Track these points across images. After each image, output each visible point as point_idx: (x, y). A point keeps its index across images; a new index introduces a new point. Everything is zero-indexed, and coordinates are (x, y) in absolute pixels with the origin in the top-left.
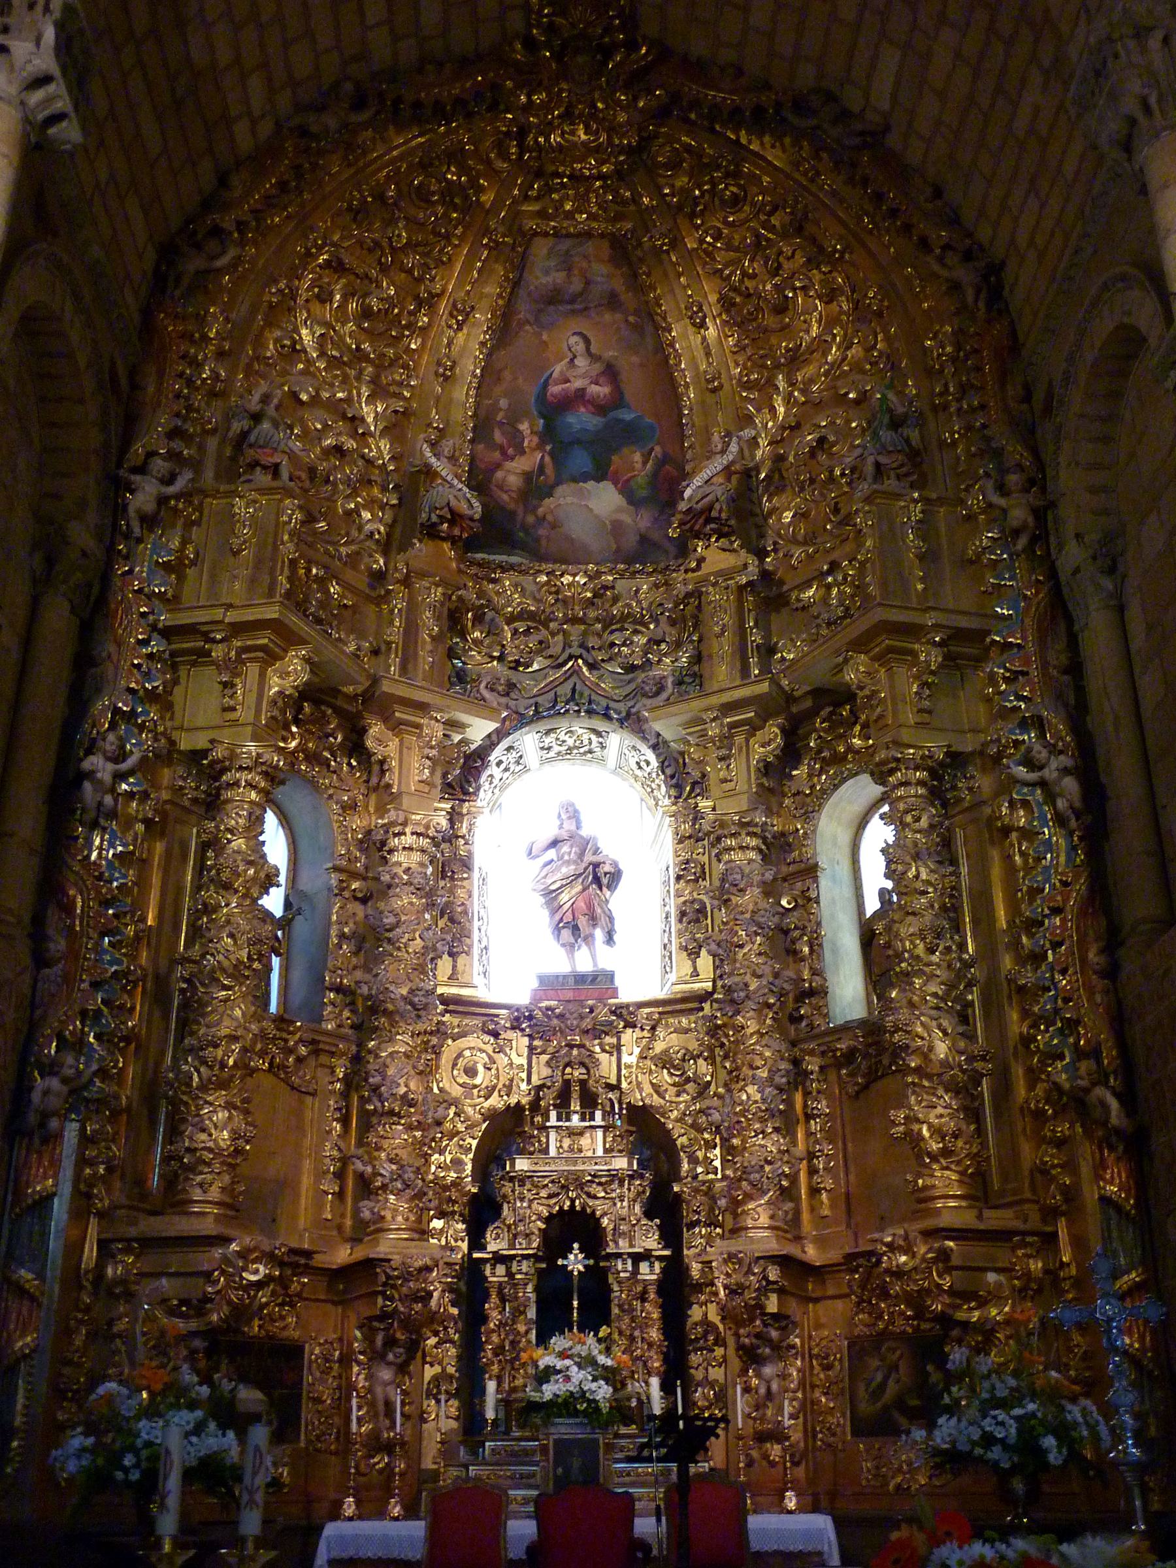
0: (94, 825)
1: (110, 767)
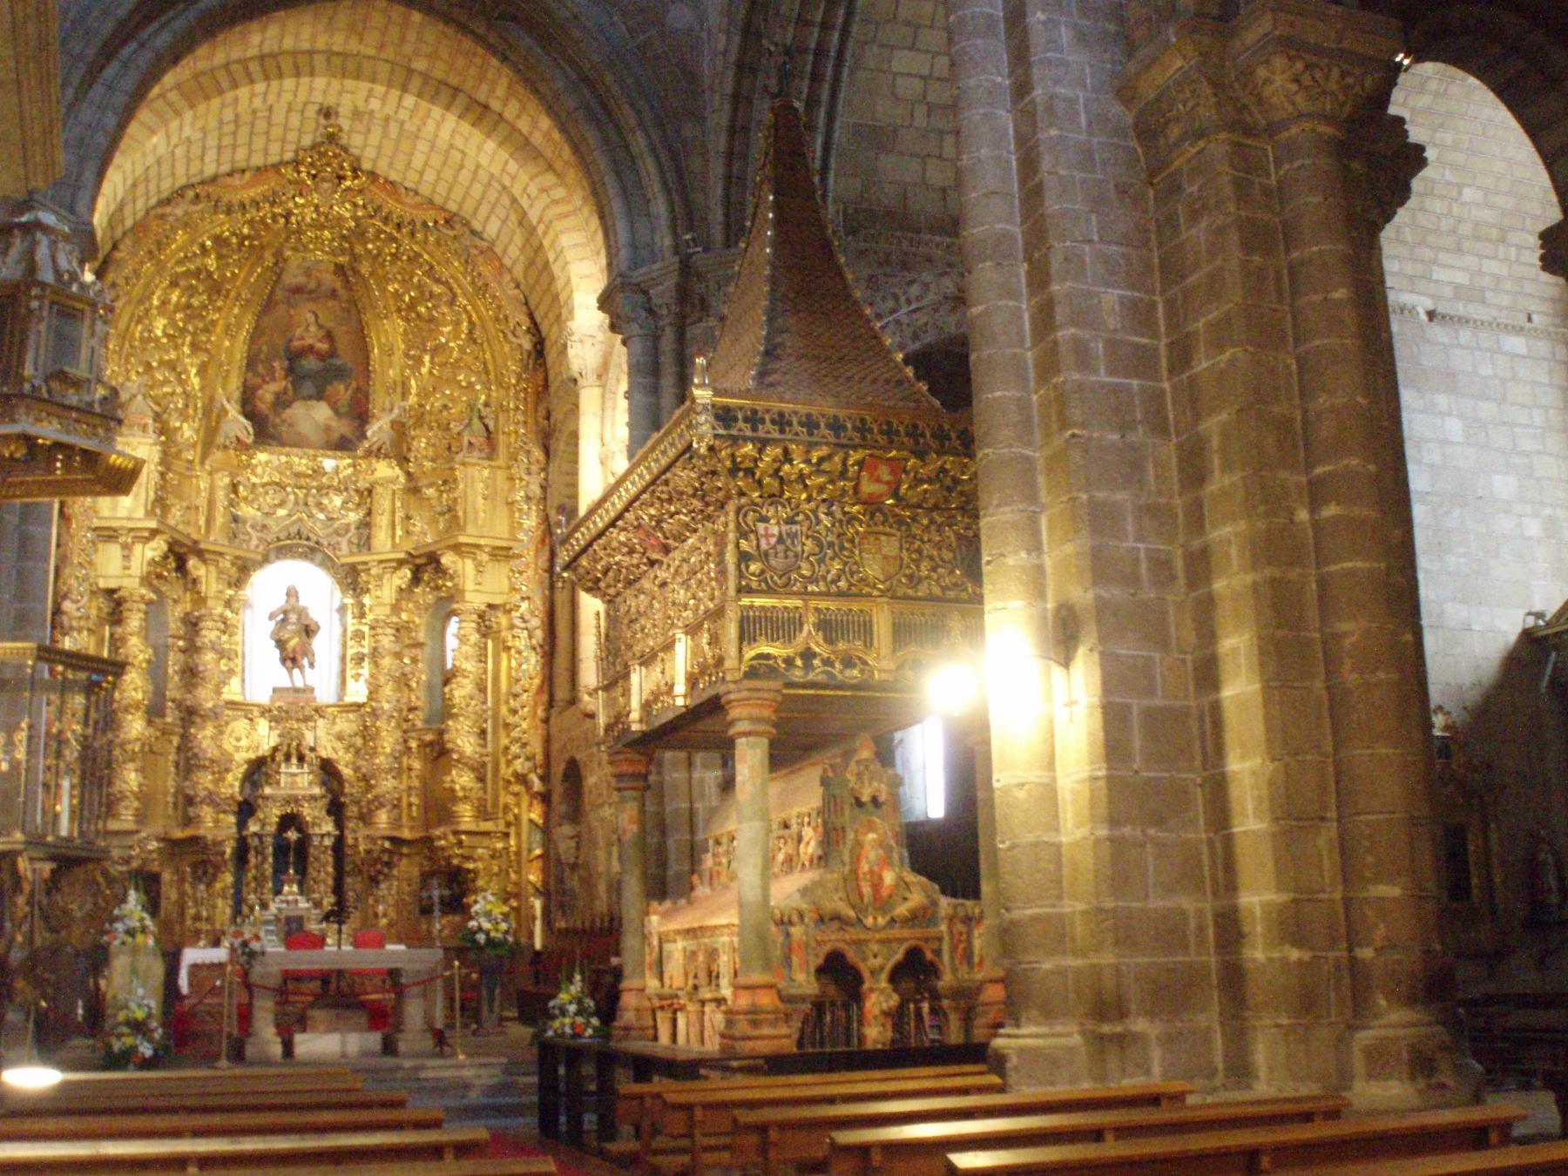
0: (65, 634)
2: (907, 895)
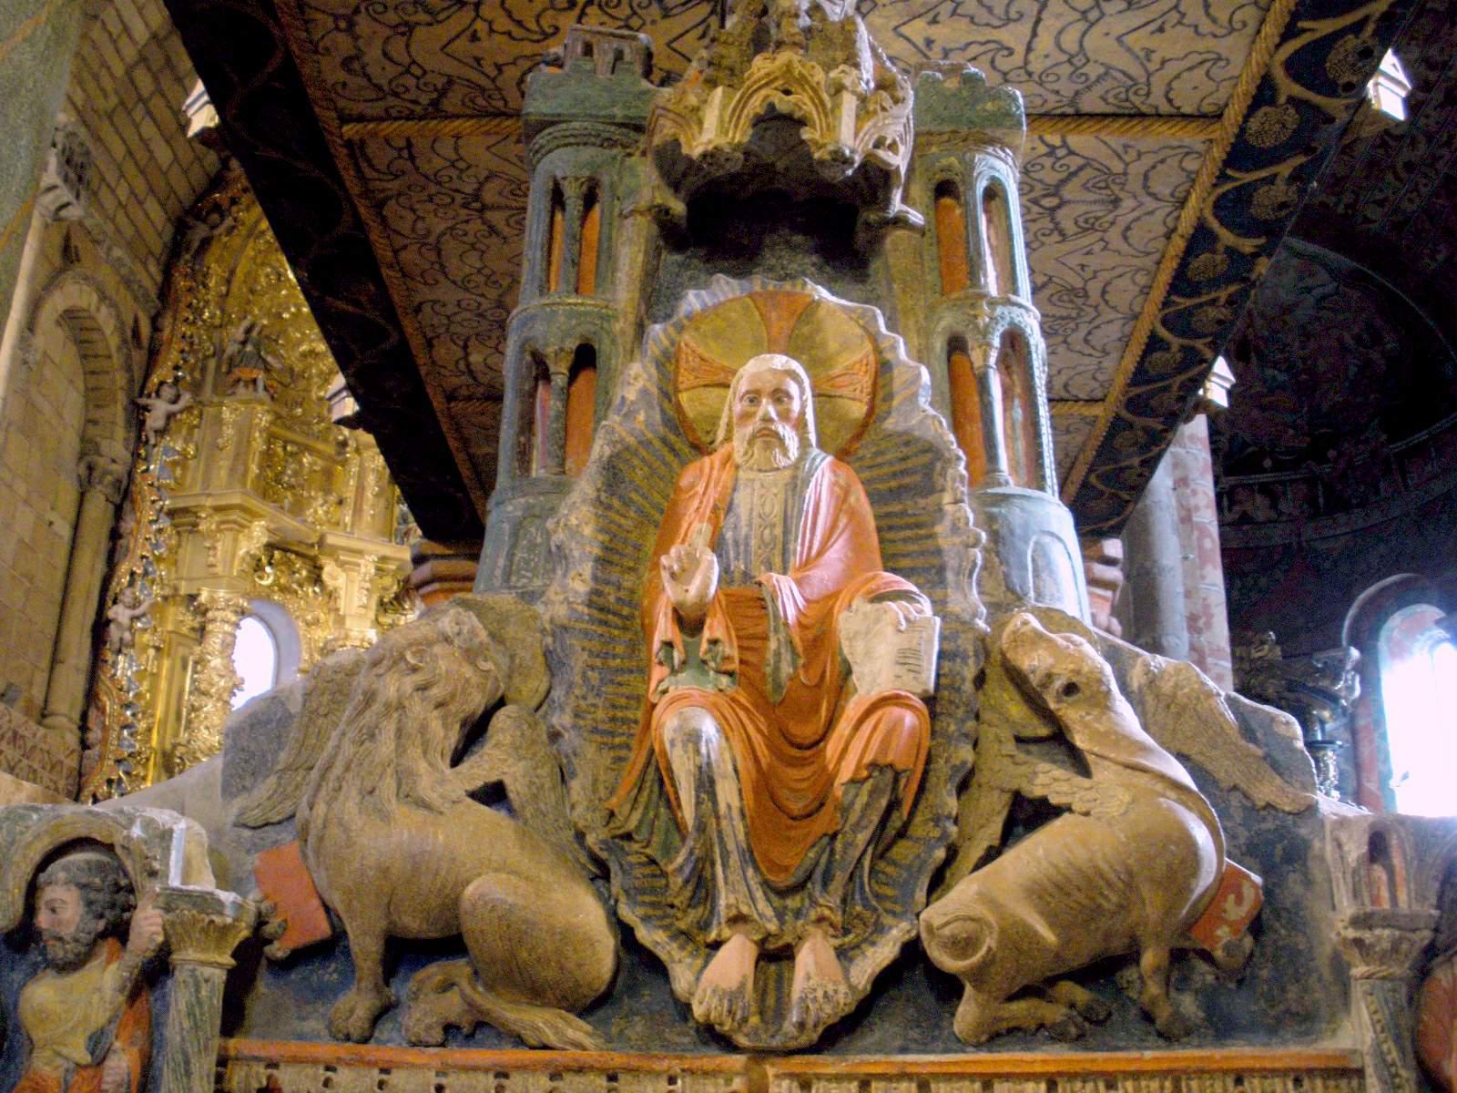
0: (119, 652)
1: (129, 613)
2: (1049, 780)
